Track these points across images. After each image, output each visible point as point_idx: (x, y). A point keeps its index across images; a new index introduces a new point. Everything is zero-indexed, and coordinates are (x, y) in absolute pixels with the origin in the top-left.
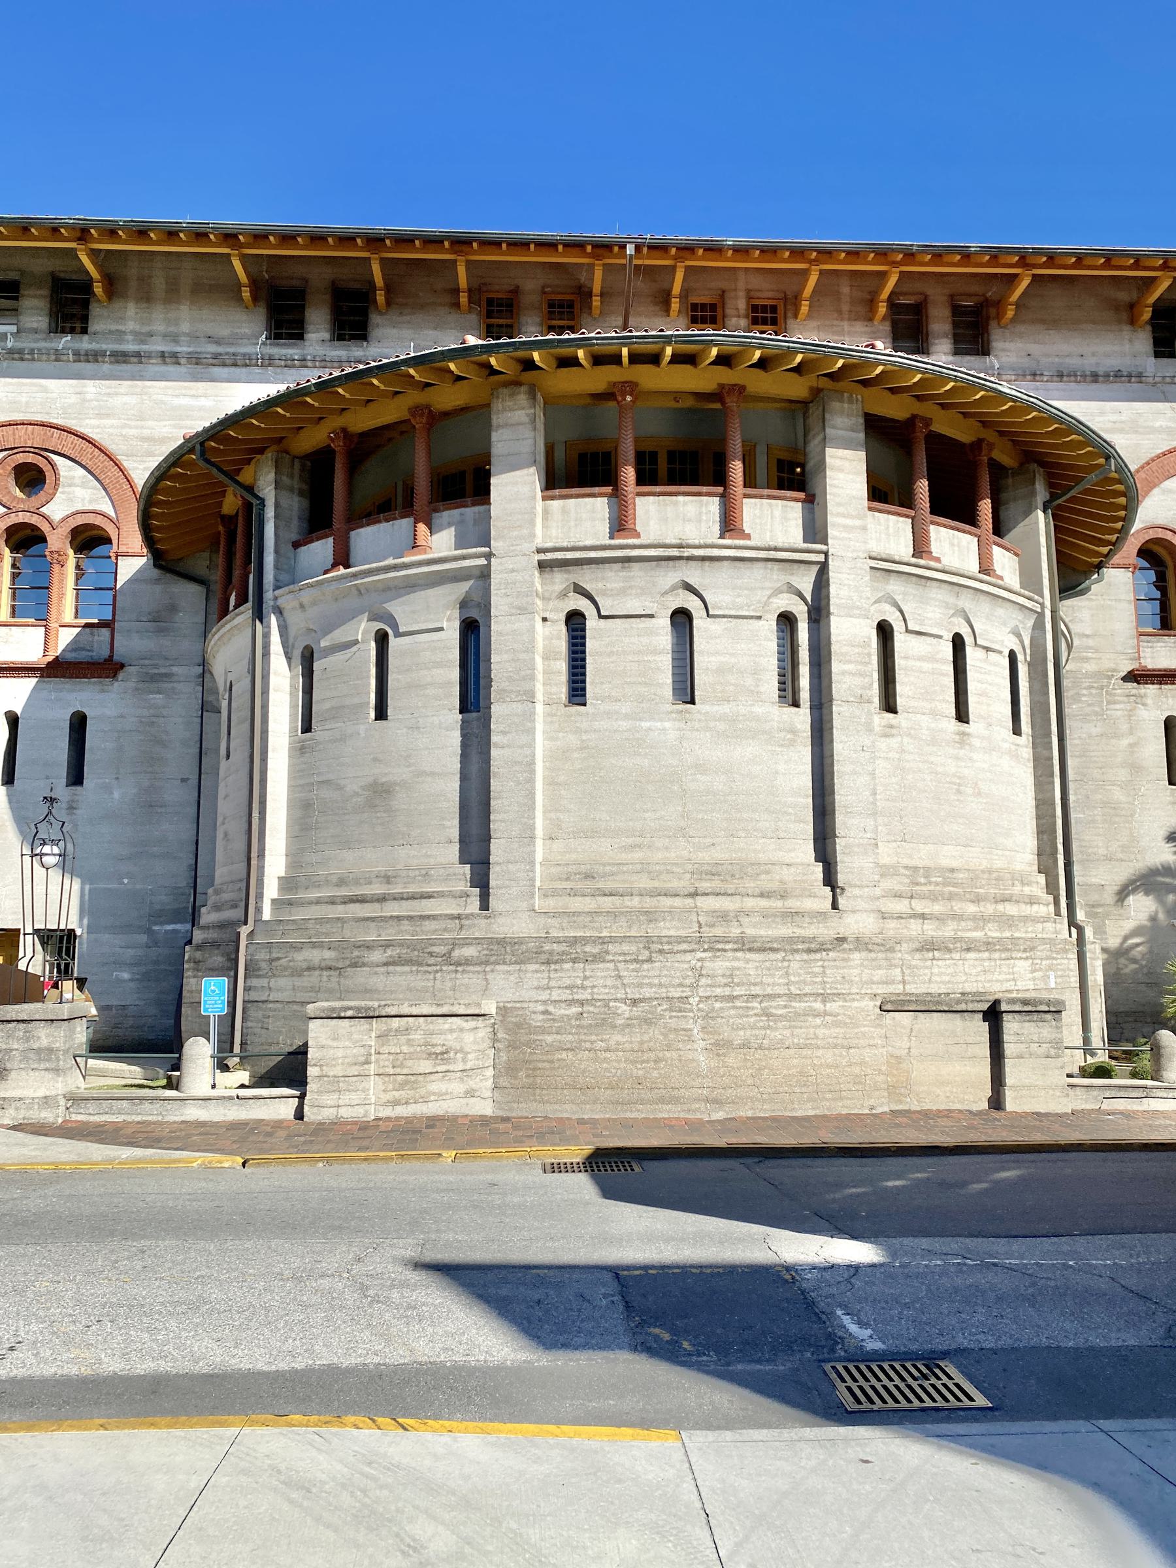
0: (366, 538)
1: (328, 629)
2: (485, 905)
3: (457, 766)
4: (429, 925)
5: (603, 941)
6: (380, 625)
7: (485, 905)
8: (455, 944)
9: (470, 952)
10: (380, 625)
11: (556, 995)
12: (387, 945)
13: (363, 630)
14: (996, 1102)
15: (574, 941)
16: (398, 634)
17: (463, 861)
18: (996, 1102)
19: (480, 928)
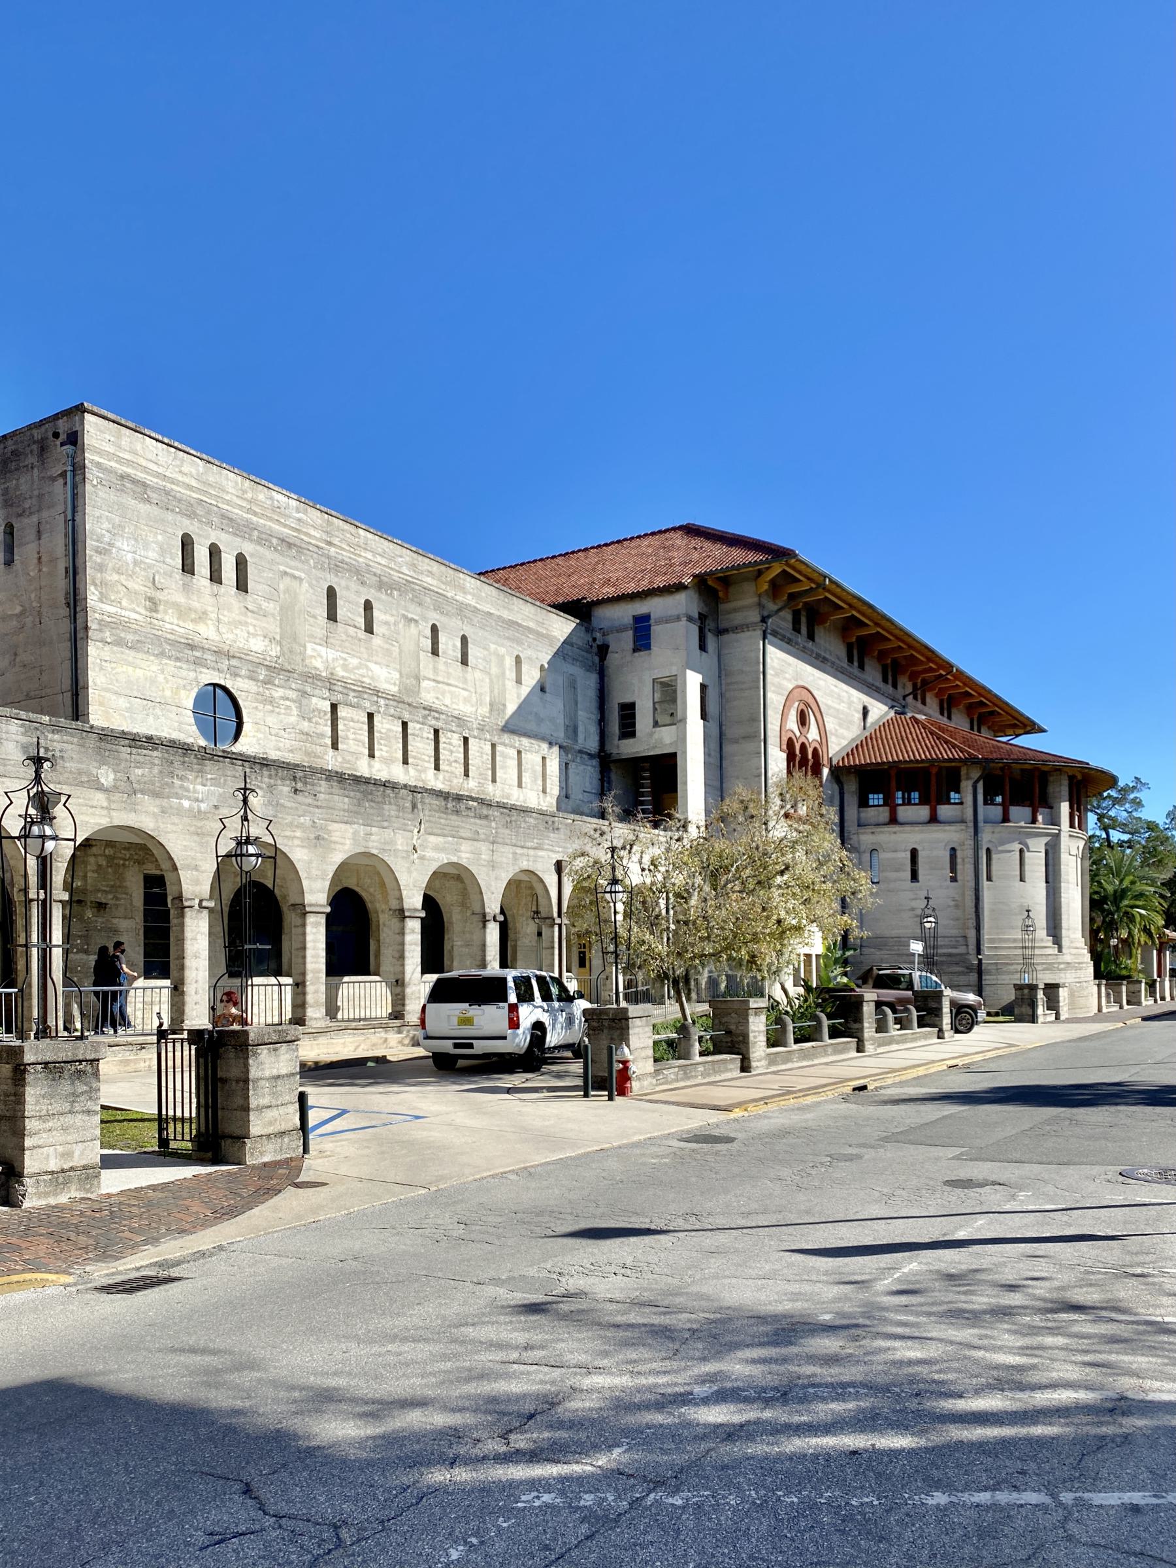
0: (1014, 811)
1: (1002, 844)
2: (1060, 950)
3: (1044, 901)
4: (1050, 957)
5: (1082, 963)
6: (1021, 846)
7: (1060, 950)
8: (1060, 963)
9: (1062, 966)
10: (1021, 846)
11: (1077, 980)
12: (1043, 964)
13: (1017, 846)
14: (1100, 1010)
15: (1079, 963)
16: (1029, 851)
17: (1048, 935)
18: (1100, 1010)
19: (1061, 959)
